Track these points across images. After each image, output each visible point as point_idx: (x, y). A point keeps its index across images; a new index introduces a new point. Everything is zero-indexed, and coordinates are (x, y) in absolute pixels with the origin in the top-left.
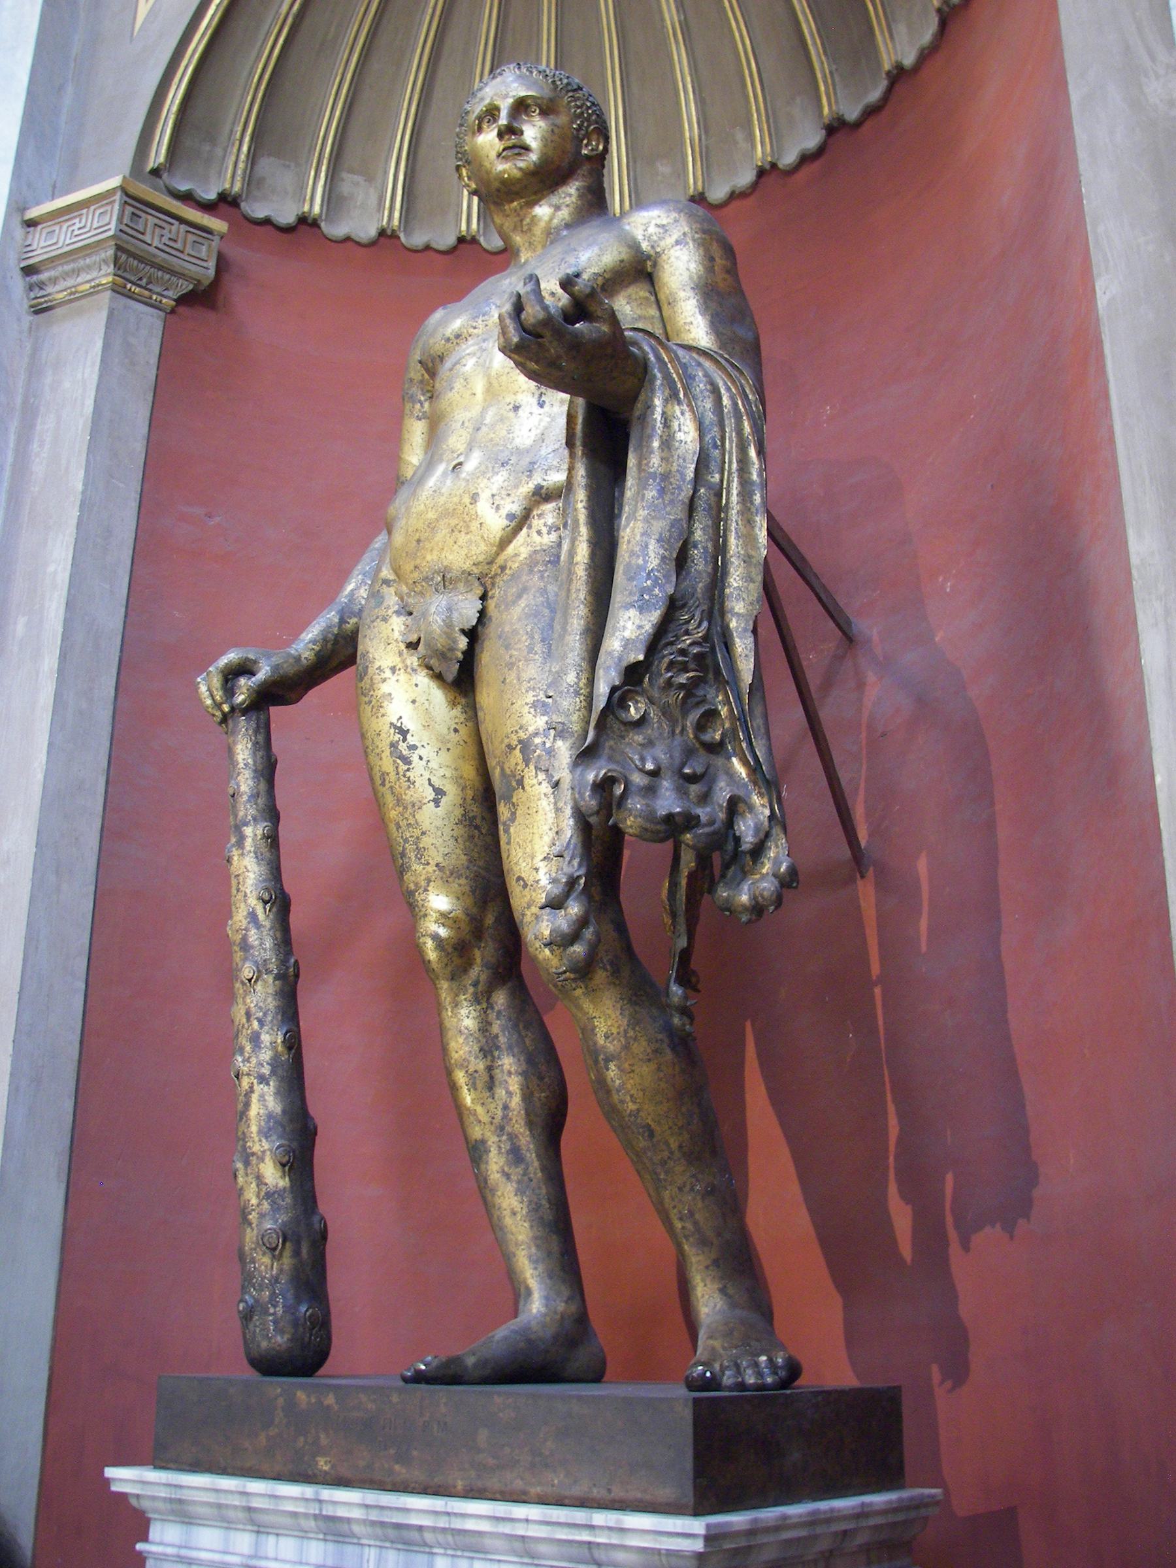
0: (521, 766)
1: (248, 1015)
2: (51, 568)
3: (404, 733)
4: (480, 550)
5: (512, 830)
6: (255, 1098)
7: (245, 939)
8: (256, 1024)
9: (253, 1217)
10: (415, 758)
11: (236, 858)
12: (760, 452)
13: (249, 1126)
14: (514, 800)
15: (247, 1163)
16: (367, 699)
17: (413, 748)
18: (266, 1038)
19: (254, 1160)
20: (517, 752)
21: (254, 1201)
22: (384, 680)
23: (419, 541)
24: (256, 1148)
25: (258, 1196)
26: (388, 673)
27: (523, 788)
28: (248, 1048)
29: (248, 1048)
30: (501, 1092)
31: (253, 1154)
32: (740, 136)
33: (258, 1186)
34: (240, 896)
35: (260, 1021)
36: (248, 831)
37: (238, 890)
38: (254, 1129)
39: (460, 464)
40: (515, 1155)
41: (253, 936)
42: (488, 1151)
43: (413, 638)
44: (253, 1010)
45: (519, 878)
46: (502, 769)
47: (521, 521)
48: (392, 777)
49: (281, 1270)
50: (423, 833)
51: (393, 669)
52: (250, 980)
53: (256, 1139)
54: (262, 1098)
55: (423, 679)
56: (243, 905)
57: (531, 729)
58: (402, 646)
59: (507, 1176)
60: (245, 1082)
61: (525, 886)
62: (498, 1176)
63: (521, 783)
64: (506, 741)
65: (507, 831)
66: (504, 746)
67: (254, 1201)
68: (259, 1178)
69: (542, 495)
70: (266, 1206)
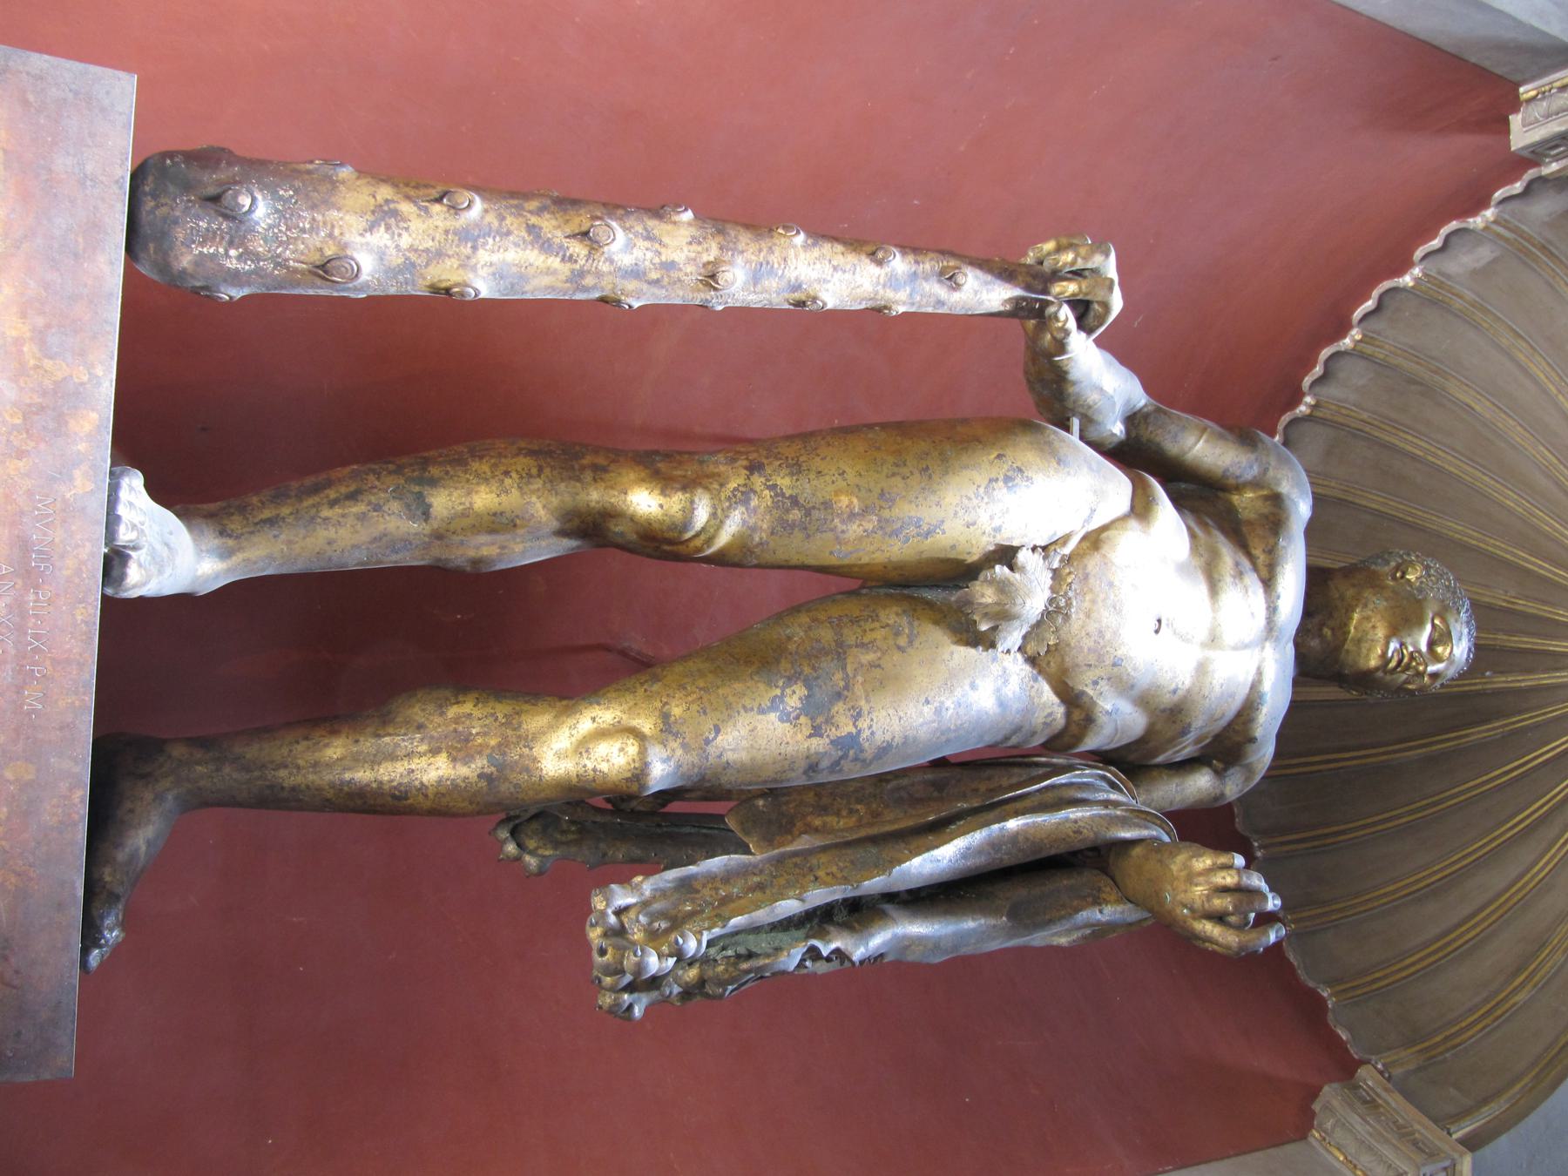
0: (834, 733)
1: (670, 266)
3: (928, 534)
5: (773, 716)
6: (555, 262)
7: (772, 272)
8: (654, 275)
9: (380, 238)
13: (516, 245)
14: (803, 719)
16: (982, 490)
18: (631, 285)
19: (467, 250)
20: (851, 729)
21: (405, 241)
22: (992, 518)
23: (1111, 585)
24: (483, 256)
25: (412, 249)
26: (996, 523)
27: (811, 736)
29: (626, 260)
30: (483, 538)
31: (475, 248)
33: (427, 251)
34: (828, 269)
35: (657, 282)
36: (902, 295)
39: (1157, 632)
41: (772, 284)
42: (412, 518)
44: (675, 274)
45: (718, 730)
46: (839, 696)
47: (1071, 698)
48: (886, 514)
49: (296, 271)
50: (808, 536)
51: (998, 530)
52: (713, 276)
53: (495, 258)
54: (549, 272)
56: (814, 275)
57: (866, 745)
58: (1015, 543)
59: (375, 540)
60: (578, 249)
62: (381, 527)
63: (816, 732)
64: (865, 708)
65: (775, 703)
66: (862, 703)
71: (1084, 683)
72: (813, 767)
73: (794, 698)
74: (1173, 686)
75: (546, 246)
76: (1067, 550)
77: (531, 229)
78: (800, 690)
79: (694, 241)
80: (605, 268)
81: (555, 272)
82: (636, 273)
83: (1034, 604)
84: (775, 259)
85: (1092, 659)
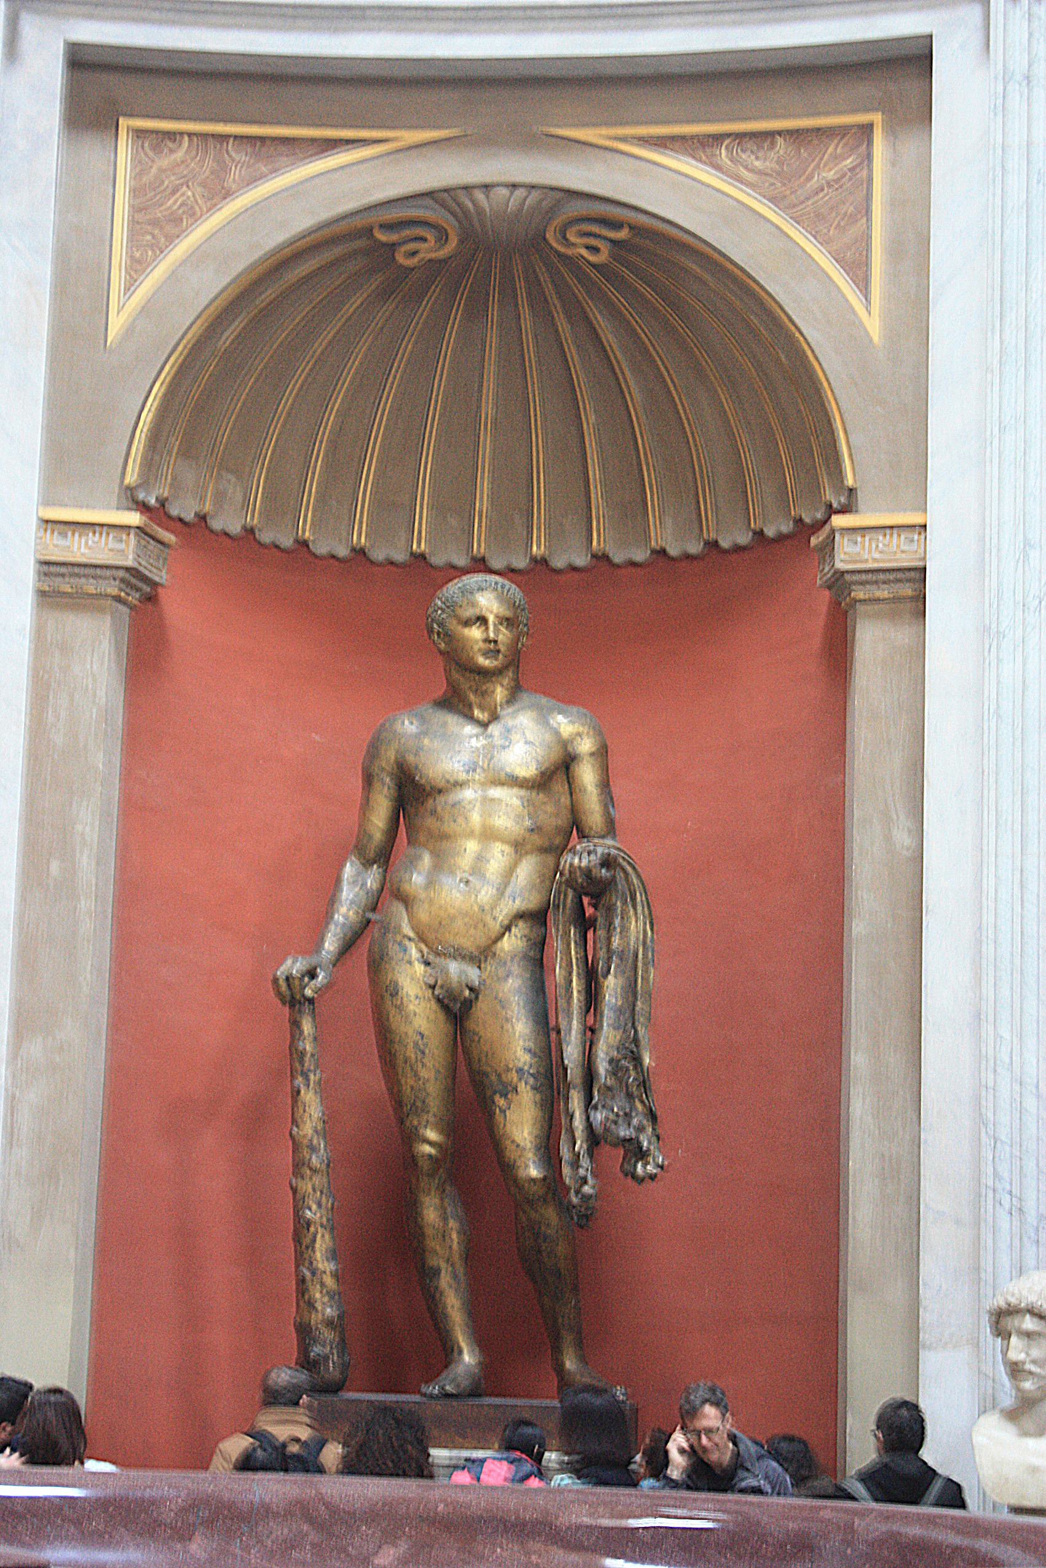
1: (314, 1190)
2: (79, 828)
3: (422, 1036)
4: (483, 941)
5: (507, 1113)
6: (319, 1236)
10: (427, 1051)
11: (303, 1092)
12: (652, 929)
15: (313, 1274)
17: (426, 1045)
21: (318, 1295)
28: (314, 1207)
29: (314, 1207)
32: (519, 520)
35: (322, 1192)
36: (312, 1077)
37: (304, 1111)
38: (318, 1255)
40: (455, 1276)
43: (432, 982)
45: (513, 1141)
55: (434, 1005)
57: (522, 1060)
59: (451, 1287)
60: (312, 1229)
61: (518, 1146)
65: (503, 1112)
67: (318, 1295)
68: (323, 1285)
69: (520, 916)
70: (326, 1299)
71: (496, 927)
72: (534, 1088)
73: (501, 1102)
74: (500, 855)
75: (314, 1240)
76: (425, 950)
77: (307, 1247)
78: (497, 1098)
79: (302, 1177)
80: (318, 1215)
81: (323, 1236)
82: (319, 1205)
83: (454, 968)
84: (305, 1142)
85: (480, 926)
